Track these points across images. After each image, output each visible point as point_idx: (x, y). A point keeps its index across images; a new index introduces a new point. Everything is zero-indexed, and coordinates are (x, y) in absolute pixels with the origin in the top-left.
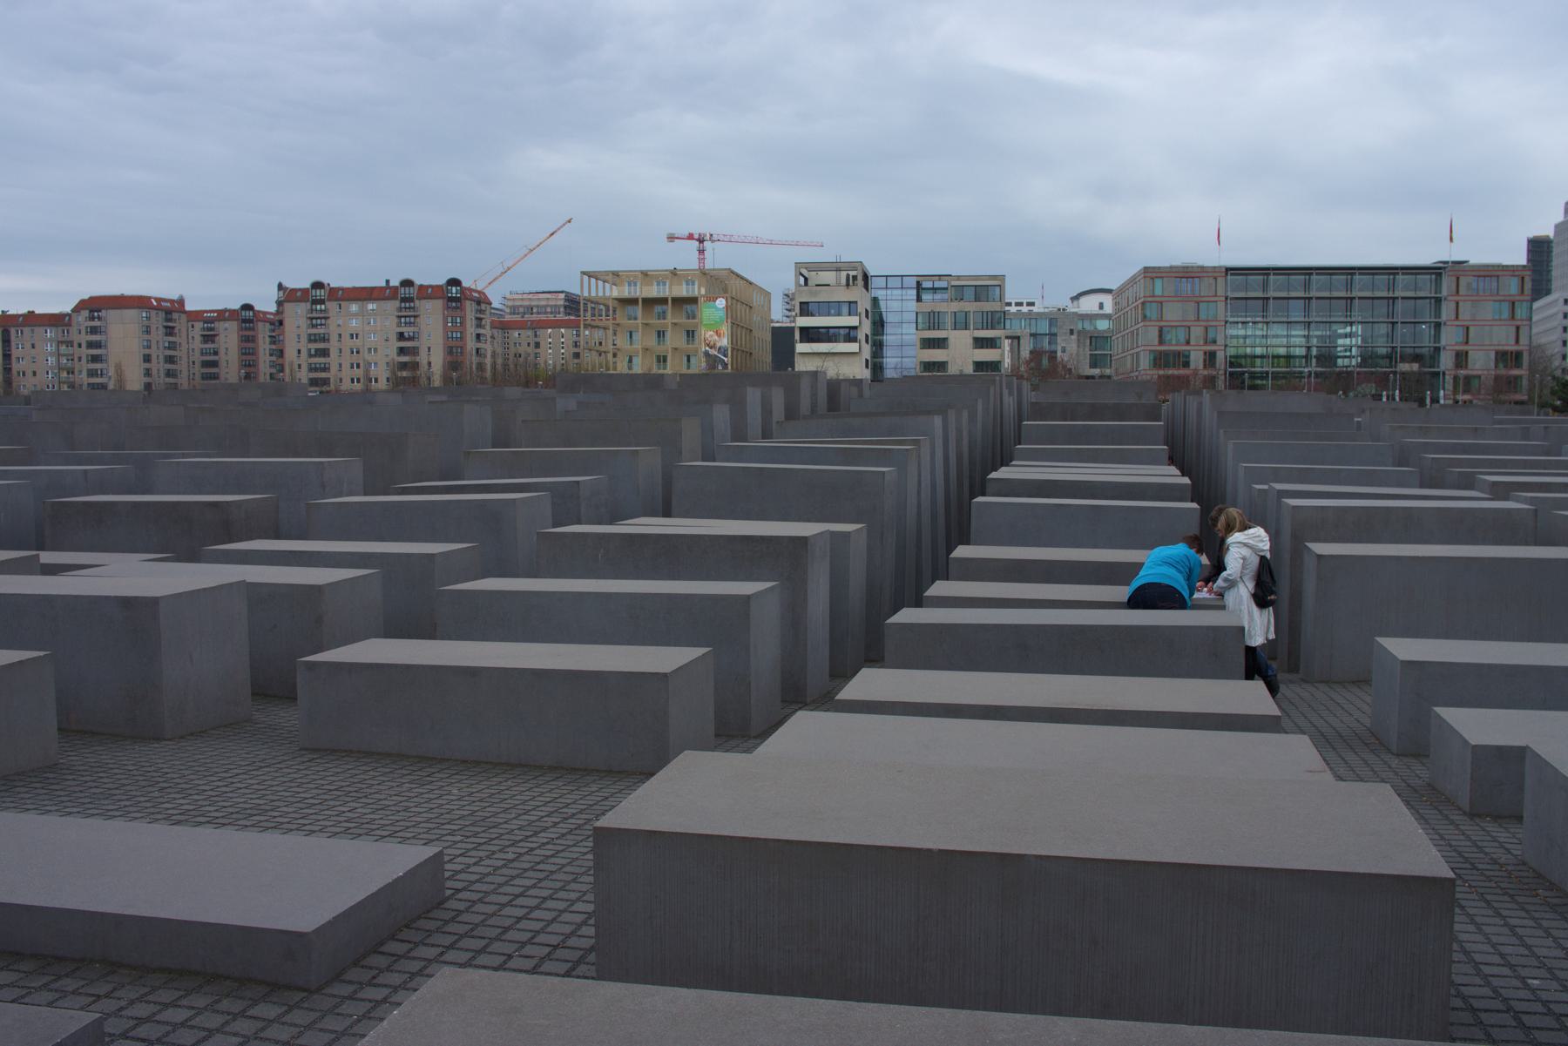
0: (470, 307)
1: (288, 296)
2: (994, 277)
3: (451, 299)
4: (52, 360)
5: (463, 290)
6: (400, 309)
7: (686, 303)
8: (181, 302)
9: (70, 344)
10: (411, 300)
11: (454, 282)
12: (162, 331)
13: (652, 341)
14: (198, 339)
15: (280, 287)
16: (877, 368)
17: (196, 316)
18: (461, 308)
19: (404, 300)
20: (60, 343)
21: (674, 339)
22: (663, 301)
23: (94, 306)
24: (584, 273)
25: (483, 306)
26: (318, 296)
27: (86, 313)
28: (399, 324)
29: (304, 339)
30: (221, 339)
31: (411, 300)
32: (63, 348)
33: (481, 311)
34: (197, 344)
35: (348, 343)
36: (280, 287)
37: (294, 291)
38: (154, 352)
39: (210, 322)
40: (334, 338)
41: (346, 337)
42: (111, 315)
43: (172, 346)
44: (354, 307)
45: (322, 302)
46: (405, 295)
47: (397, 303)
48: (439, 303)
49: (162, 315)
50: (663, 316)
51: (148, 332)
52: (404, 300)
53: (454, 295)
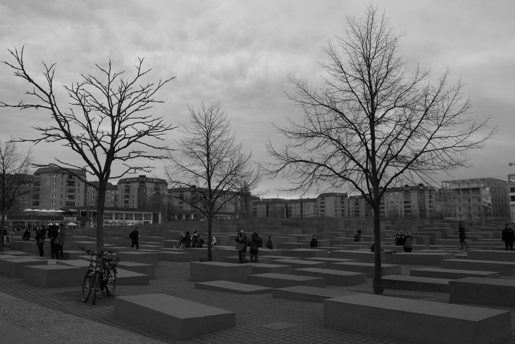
0: (427, 194)
3: (420, 190)
5: (424, 187)
7: (477, 190)
9: (317, 207)
12: (340, 202)
13: (467, 202)
14: (354, 204)
16: (302, 217)
18: (424, 193)
19: (406, 191)
21: (474, 201)
24: (443, 182)
25: (432, 192)
27: (320, 198)
28: (405, 198)
31: (408, 191)
34: (354, 206)
35: (390, 205)
38: (337, 208)
40: (386, 203)
41: (389, 203)
43: (343, 207)
49: (340, 198)
50: (469, 194)
51: (336, 203)
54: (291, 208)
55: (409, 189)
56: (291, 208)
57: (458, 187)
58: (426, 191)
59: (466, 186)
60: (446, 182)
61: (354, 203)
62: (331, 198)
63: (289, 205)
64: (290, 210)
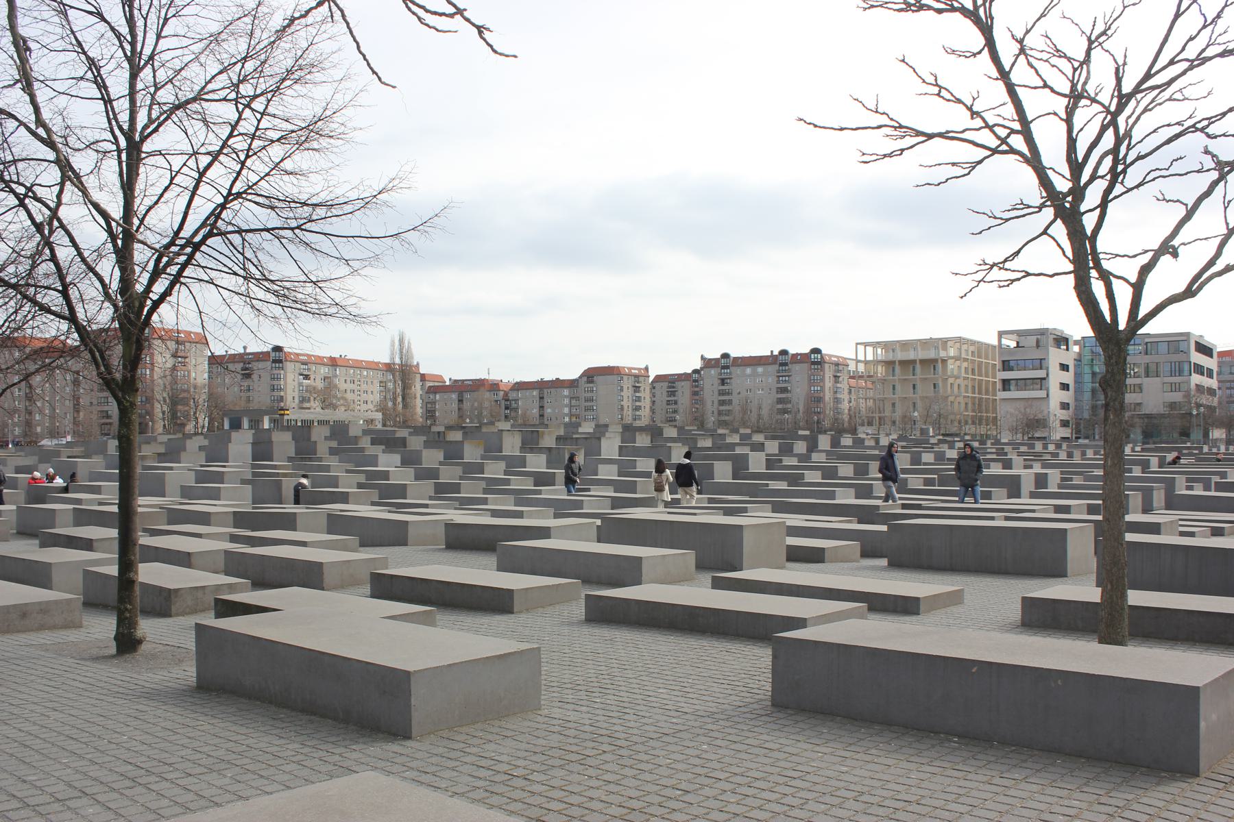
1: (708, 363)
2: (1181, 334)
3: (814, 363)
4: (566, 410)
8: (647, 369)
9: (577, 398)
10: (785, 364)
11: (816, 351)
12: (631, 390)
14: (665, 394)
15: (702, 357)
17: (659, 378)
18: (822, 370)
19: (782, 364)
20: (571, 398)
22: (913, 362)
23: (591, 375)
25: (841, 368)
26: (724, 365)
27: (585, 379)
28: (778, 382)
29: (716, 393)
30: (679, 393)
31: (785, 364)
32: (574, 402)
33: (839, 371)
36: (702, 357)
37: (710, 360)
39: (670, 382)
40: (735, 393)
43: (639, 399)
44: (749, 370)
45: (727, 367)
46: (782, 361)
47: (776, 367)
48: (805, 366)
52: (782, 364)
53: (814, 359)
54: (516, 400)
55: (729, 362)
56: (516, 400)
57: (890, 357)
58: (827, 366)
59: (911, 355)
60: (866, 345)
61: (665, 389)
63: (512, 395)
64: (514, 405)
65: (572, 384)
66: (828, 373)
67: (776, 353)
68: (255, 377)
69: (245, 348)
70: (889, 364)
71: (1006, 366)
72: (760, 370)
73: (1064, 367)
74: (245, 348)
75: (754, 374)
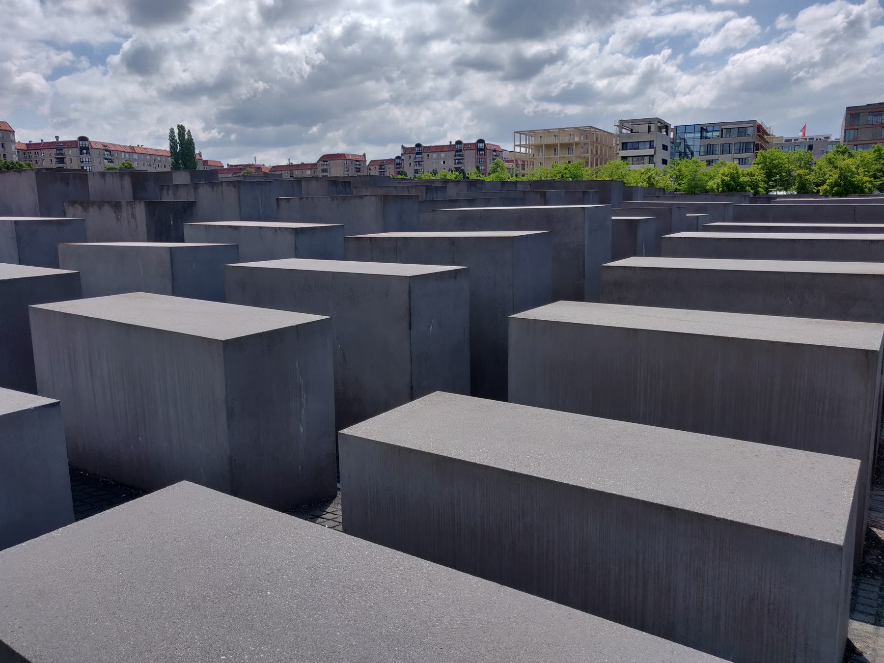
6: (455, 156)
8: (364, 155)
10: (460, 151)
17: (373, 162)
19: (457, 151)
23: (326, 158)
31: (460, 151)
42: (331, 162)
44: (435, 155)
62: (339, 162)
65: (312, 166)
66: (489, 158)
67: (453, 143)
68: (67, 160)
69: (57, 137)
70: (538, 147)
71: (625, 146)
72: (443, 155)
73: (665, 148)
74: (57, 137)
75: (439, 158)
